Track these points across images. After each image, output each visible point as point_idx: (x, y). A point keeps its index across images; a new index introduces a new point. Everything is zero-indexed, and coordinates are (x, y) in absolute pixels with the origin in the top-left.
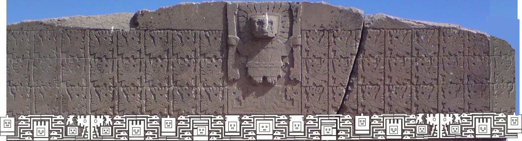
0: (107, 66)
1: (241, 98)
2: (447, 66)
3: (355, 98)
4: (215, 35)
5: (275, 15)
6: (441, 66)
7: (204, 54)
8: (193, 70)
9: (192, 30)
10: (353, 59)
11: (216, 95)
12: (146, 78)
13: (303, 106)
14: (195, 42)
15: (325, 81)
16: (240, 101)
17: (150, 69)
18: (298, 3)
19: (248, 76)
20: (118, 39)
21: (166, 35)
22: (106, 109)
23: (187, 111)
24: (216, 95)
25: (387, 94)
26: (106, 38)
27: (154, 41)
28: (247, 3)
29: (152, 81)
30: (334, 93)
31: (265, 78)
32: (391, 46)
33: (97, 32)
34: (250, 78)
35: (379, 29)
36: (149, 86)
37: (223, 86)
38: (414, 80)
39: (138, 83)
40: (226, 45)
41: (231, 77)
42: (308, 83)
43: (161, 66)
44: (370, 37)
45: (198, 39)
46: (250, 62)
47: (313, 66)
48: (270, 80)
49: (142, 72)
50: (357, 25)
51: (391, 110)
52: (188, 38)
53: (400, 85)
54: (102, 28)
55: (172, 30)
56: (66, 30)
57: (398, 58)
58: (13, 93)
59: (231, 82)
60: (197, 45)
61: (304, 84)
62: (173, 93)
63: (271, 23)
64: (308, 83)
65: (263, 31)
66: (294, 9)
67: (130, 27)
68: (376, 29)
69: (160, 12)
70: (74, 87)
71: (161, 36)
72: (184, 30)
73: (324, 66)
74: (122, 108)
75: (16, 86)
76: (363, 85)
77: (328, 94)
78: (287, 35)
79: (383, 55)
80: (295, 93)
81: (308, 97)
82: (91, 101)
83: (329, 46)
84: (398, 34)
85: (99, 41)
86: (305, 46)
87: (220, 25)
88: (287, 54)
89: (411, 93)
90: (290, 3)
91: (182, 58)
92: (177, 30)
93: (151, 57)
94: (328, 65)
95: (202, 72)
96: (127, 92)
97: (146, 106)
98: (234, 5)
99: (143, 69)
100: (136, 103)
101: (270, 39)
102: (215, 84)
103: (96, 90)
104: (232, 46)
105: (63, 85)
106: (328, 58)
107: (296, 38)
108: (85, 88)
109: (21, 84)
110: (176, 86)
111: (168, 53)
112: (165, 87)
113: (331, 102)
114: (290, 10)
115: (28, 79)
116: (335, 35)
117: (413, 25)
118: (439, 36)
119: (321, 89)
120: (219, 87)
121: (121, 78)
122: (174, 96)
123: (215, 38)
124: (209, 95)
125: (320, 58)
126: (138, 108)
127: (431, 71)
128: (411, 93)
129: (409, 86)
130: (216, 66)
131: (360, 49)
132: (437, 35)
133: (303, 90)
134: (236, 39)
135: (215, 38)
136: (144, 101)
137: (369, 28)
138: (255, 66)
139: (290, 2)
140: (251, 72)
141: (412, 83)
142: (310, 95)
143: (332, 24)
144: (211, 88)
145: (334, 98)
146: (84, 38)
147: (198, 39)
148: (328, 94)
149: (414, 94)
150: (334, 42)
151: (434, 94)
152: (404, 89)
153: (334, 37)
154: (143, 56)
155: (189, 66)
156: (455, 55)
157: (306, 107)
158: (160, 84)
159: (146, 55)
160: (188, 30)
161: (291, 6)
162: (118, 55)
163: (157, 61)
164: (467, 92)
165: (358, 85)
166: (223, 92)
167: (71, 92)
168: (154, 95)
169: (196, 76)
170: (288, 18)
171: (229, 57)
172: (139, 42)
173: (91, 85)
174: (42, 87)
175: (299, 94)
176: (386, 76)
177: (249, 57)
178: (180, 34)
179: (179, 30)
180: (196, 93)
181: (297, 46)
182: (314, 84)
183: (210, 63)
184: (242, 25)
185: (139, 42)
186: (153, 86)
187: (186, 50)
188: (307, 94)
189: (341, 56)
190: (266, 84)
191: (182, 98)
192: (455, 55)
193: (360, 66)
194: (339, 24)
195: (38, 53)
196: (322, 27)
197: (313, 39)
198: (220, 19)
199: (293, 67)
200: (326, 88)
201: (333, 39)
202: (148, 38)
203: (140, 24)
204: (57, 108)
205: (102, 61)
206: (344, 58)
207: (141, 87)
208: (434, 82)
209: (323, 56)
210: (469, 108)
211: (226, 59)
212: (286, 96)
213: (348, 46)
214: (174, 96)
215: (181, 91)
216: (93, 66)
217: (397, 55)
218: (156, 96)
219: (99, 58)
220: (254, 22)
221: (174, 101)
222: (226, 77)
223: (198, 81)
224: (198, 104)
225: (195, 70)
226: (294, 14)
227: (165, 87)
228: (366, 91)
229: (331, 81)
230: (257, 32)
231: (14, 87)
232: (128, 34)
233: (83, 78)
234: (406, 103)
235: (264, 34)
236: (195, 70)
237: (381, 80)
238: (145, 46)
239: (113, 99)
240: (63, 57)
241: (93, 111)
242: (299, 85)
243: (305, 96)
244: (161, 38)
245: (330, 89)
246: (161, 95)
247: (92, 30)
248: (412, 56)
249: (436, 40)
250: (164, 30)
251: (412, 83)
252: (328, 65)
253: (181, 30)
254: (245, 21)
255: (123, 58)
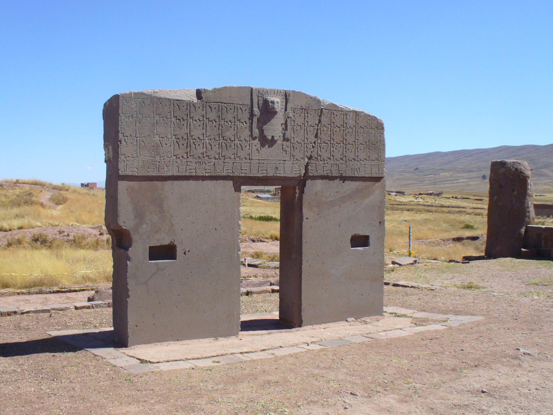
0: (183, 125)
1: (259, 149)
2: (359, 134)
3: (316, 151)
4: (245, 108)
5: (278, 98)
6: (357, 133)
7: (240, 120)
8: (233, 130)
9: (233, 104)
10: (316, 128)
11: (246, 146)
12: (206, 134)
13: (292, 155)
14: (234, 112)
15: (303, 140)
16: (258, 150)
17: (208, 128)
18: (290, 91)
19: (263, 135)
20: (190, 107)
21: (218, 105)
22: (183, 154)
23: (229, 156)
24: (246, 146)
25: (332, 149)
26: (183, 106)
27: (211, 110)
28: (263, 89)
29: (210, 136)
30: (307, 148)
31: (273, 137)
32: (334, 121)
33: (178, 102)
34: (265, 136)
35: (328, 110)
36: (208, 140)
37: (250, 141)
38: (345, 141)
39: (201, 137)
40: (252, 115)
41: (254, 135)
42: (294, 141)
43: (215, 126)
44: (324, 115)
45: (236, 110)
46: (265, 126)
47: (296, 130)
48: (275, 138)
49: (204, 130)
50: (319, 107)
51: (333, 159)
52: (231, 109)
53: (338, 144)
54: (181, 99)
55: (221, 103)
56: (159, 99)
57: (337, 128)
58: (126, 142)
59: (254, 139)
60: (236, 113)
61: (292, 141)
62: (222, 145)
63: (278, 103)
64: (294, 141)
65: (274, 108)
66: (288, 95)
67: (198, 99)
68: (327, 110)
69: (215, 91)
70: (163, 139)
71: (215, 106)
72: (228, 103)
73: (303, 130)
74: (192, 154)
75: (127, 137)
76: (320, 143)
77: (304, 148)
78: (283, 110)
79: (330, 126)
80: (287, 147)
81: (294, 150)
82: (174, 149)
83: (305, 119)
84: (337, 114)
85: (179, 108)
86: (293, 118)
87: (249, 103)
88: (284, 123)
89: (343, 149)
90: (285, 91)
91: (227, 122)
92: (224, 103)
93: (210, 120)
94: (304, 130)
95: (238, 131)
96: (195, 143)
97: (206, 152)
98: (256, 89)
99: (205, 128)
100: (200, 150)
101: (276, 113)
102: (245, 139)
103: (177, 141)
104: (255, 115)
105: (157, 137)
106: (305, 126)
107: (289, 113)
108: (170, 139)
109: (131, 135)
110: (224, 140)
111: (219, 118)
112: (217, 140)
113: (306, 153)
114: (286, 95)
115: (135, 132)
116: (308, 112)
117: (344, 109)
118: (356, 116)
119: (301, 145)
120: (247, 141)
121: (192, 134)
122: (222, 146)
123: (246, 110)
124: (242, 146)
125: (300, 126)
126: (202, 153)
127: (352, 136)
128: (343, 149)
129: (342, 145)
130: (246, 128)
131: (320, 121)
132: (355, 115)
133: (292, 144)
134: (258, 111)
135: (246, 110)
136: (205, 149)
137: (324, 109)
138: (268, 129)
139: (286, 90)
140: (266, 133)
141: (343, 143)
142: (295, 148)
143: (306, 105)
144: (243, 142)
145: (307, 151)
146: (170, 105)
147: (236, 110)
148: (304, 148)
149: (344, 150)
150: (307, 116)
151: (354, 150)
152: (340, 146)
153: (308, 113)
154: (205, 119)
155: (231, 127)
156: (363, 128)
157: (293, 156)
158: (214, 138)
159: (207, 119)
160: (230, 103)
161: (286, 93)
162: (190, 118)
163: (213, 123)
164: (368, 150)
165: (318, 143)
166: (249, 145)
167: (162, 142)
168: (211, 145)
169: (235, 134)
170: (284, 101)
171: (253, 122)
172: (203, 110)
173: (174, 137)
174: (144, 138)
175: (290, 147)
176: (332, 138)
177: (265, 123)
178: (226, 106)
179: (226, 103)
180: (235, 145)
181: (289, 118)
182: (297, 142)
183: (242, 125)
184: (261, 102)
185: (203, 110)
186: (210, 140)
187: (229, 117)
188: (294, 148)
189: (311, 125)
190: (272, 142)
191: (227, 148)
192: (363, 128)
193: (319, 131)
194: (310, 105)
195: (142, 114)
196: (301, 106)
197: (297, 114)
198: (249, 98)
199: (287, 131)
200: (303, 144)
201: (307, 114)
202: (208, 107)
203: (204, 98)
204: (153, 153)
205: (180, 122)
206: (312, 126)
207: (203, 140)
208: (354, 143)
209: (302, 125)
210: (369, 159)
211: (252, 123)
212: (283, 148)
213: (313, 119)
214: (222, 146)
215: (226, 143)
216: (175, 125)
217: (337, 126)
218: (212, 147)
219: (179, 120)
220: (268, 101)
221: (222, 150)
222: (251, 135)
223: (236, 137)
224: (236, 153)
225: (234, 130)
226: (288, 97)
227: (217, 140)
228: (322, 147)
229: (306, 140)
230: (270, 108)
231: (126, 137)
232: (196, 104)
233: (169, 132)
234: (341, 155)
235: (275, 110)
236: (234, 130)
237: (329, 141)
238: (206, 113)
239: (187, 147)
240: (157, 118)
241: (175, 155)
242: (289, 142)
243: (292, 148)
244: (215, 108)
245: (305, 145)
246: (215, 145)
247: (175, 100)
248: (344, 127)
249: (355, 118)
250: (217, 102)
251: (343, 143)
252: (304, 130)
253: (226, 103)
254: (262, 100)
255: (193, 120)
